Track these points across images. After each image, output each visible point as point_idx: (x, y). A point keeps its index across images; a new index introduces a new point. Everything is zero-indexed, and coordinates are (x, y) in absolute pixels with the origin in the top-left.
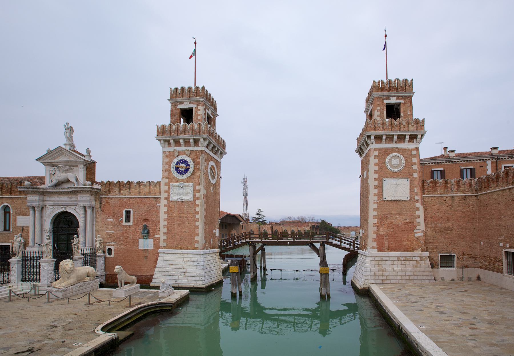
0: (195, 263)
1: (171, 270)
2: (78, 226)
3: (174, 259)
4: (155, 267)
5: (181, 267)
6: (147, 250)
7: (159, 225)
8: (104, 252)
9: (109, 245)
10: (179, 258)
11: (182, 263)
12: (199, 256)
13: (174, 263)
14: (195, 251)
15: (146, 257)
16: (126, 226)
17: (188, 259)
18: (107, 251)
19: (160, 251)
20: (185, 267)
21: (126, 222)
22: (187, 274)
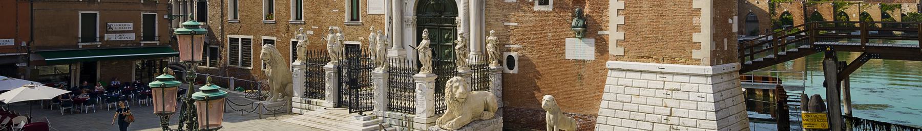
0: (693, 96)
1: (635, 107)
2: (456, 13)
3: (643, 84)
4: (599, 99)
5: (659, 101)
6: (584, 61)
7: (606, 8)
8: (502, 65)
9: (509, 50)
10: (655, 82)
11: (660, 93)
12: (703, 80)
13: (643, 92)
14: (692, 68)
15: (581, 77)
16: (539, 12)
17: (677, 86)
18: (505, 62)
19: (610, 64)
20: (670, 103)
21: (540, 4)
22: (673, 120)
